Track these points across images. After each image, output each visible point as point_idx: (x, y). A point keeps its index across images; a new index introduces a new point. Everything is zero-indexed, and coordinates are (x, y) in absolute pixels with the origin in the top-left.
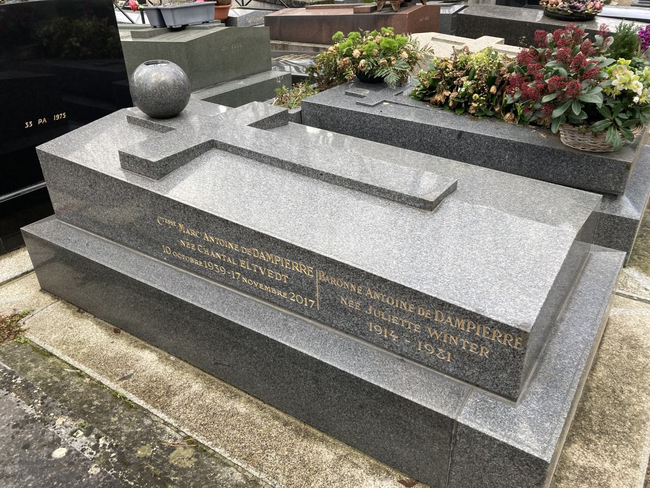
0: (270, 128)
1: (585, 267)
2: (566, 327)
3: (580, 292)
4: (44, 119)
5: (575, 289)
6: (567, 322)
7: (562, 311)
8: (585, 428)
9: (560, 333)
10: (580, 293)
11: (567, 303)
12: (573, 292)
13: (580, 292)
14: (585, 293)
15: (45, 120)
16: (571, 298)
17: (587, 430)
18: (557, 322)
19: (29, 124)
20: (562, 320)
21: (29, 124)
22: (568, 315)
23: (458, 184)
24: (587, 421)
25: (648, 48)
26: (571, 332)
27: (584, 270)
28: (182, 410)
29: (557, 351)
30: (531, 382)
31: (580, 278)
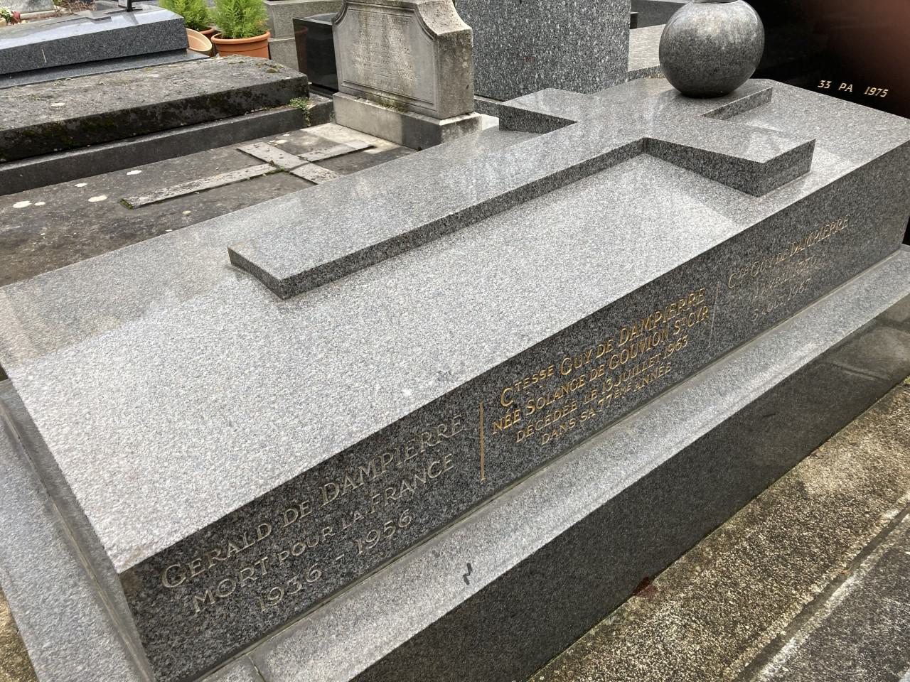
0: (701, 173)
1: (125, 649)
2: (32, 510)
3: (75, 585)
4: (851, 85)
5: (88, 578)
6: (38, 516)
7: (62, 521)
8: (11, 655)
9: (31, 495)
10: (71, 582)
11: (69, 541)
12: (84, 569)
13: (75, 585)
14: (64, 593)
15: (851, 88)
16: (74, 555)
17: (8, 656)
18: (49, 501)
19: (825, 83)
20: (48, 511)
21: (825, 83)
22: (49, 528)
23: (233, 248)
24: (16, 667)
25: (12, 12)
26: (20, 513)
27: (118, 637)
28: (459, 496)
29: (12, 475)
30: (5, 423)
31: (104, 611)
